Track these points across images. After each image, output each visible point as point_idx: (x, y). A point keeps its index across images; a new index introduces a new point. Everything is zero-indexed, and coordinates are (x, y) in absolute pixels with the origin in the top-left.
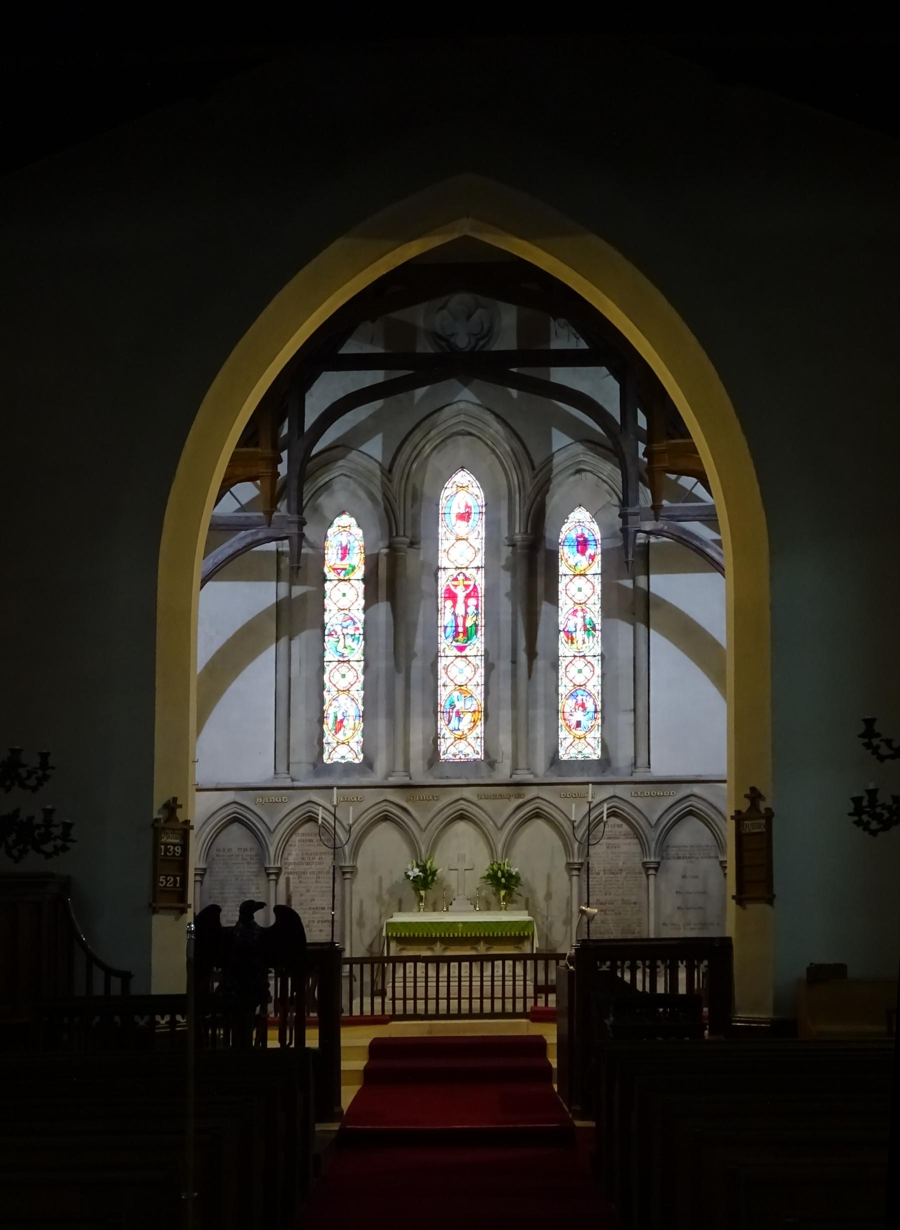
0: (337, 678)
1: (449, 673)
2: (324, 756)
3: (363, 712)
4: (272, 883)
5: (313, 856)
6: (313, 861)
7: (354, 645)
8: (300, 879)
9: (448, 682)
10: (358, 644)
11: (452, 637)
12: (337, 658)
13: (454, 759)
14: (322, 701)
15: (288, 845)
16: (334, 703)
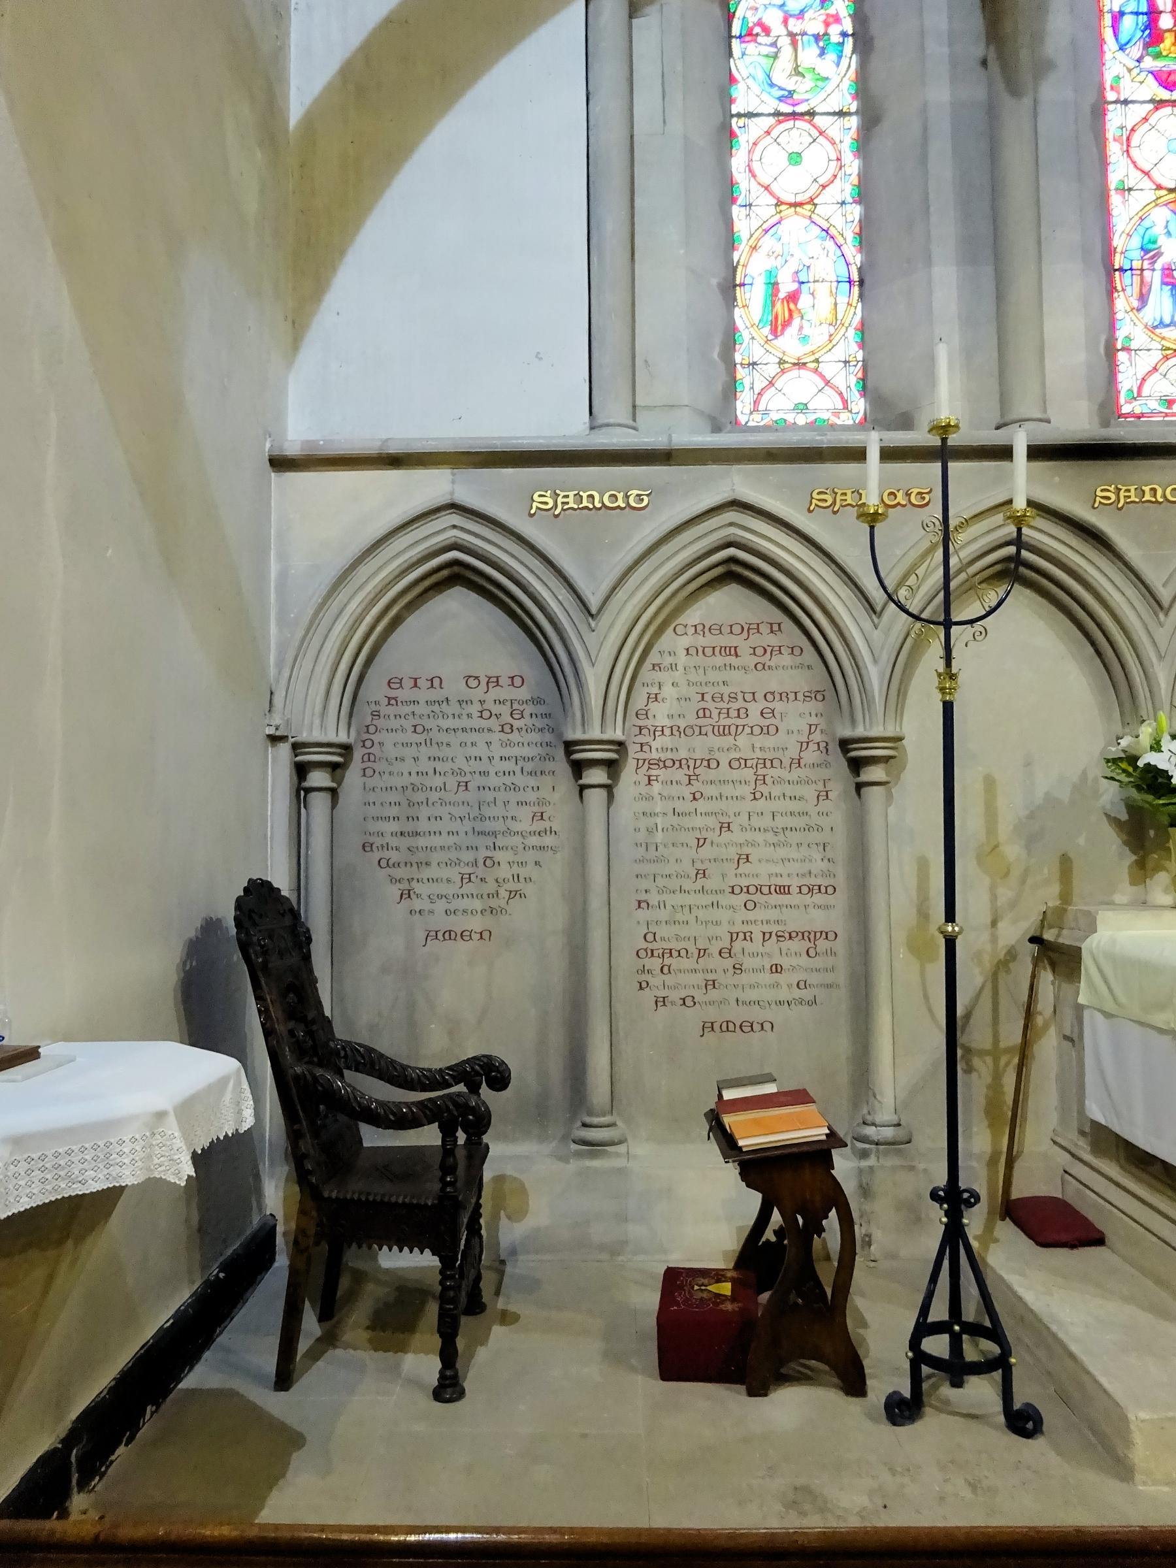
0: (772, 162)
1: (1133, 152)
2: (739, 404)
3: (860, 270)
4: (596, 798)
5: (740, 703)
6: (739, 722)
7: (826, 66)
8: (697, 786)
9: (1134, 178)
10: (838, 65)
11: (1140, 44)
12: (771, 105)
13: (1167, 415)
14: (730, 242)
15: (647, 665)
16: (767, 242)
